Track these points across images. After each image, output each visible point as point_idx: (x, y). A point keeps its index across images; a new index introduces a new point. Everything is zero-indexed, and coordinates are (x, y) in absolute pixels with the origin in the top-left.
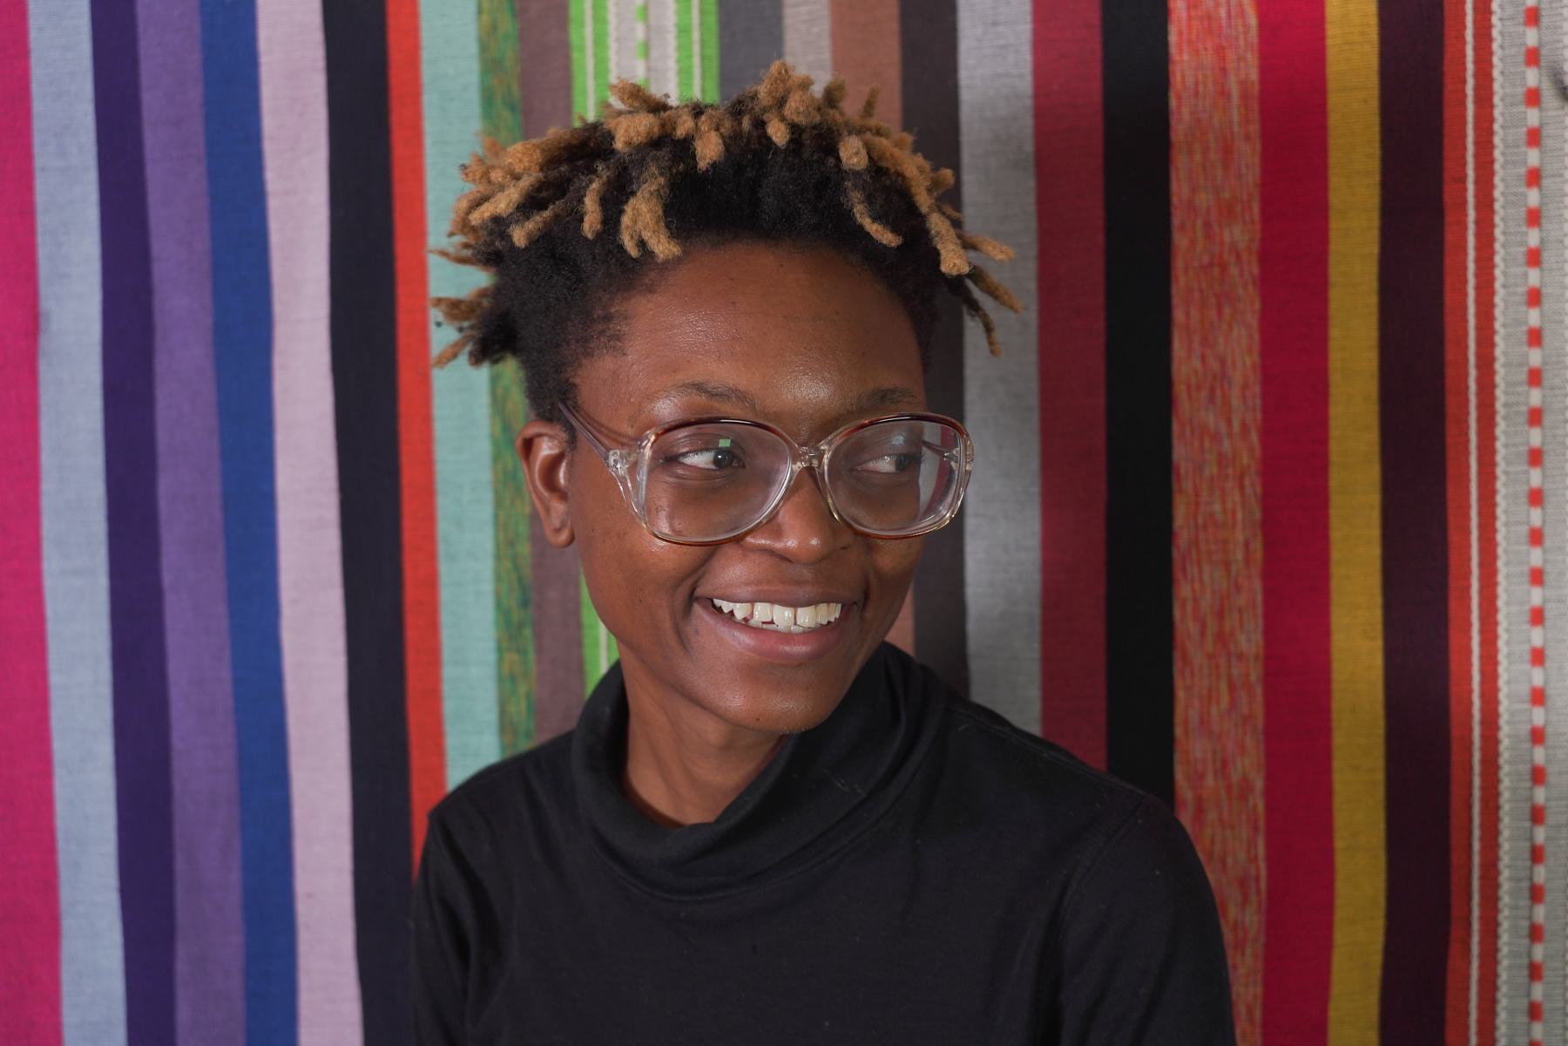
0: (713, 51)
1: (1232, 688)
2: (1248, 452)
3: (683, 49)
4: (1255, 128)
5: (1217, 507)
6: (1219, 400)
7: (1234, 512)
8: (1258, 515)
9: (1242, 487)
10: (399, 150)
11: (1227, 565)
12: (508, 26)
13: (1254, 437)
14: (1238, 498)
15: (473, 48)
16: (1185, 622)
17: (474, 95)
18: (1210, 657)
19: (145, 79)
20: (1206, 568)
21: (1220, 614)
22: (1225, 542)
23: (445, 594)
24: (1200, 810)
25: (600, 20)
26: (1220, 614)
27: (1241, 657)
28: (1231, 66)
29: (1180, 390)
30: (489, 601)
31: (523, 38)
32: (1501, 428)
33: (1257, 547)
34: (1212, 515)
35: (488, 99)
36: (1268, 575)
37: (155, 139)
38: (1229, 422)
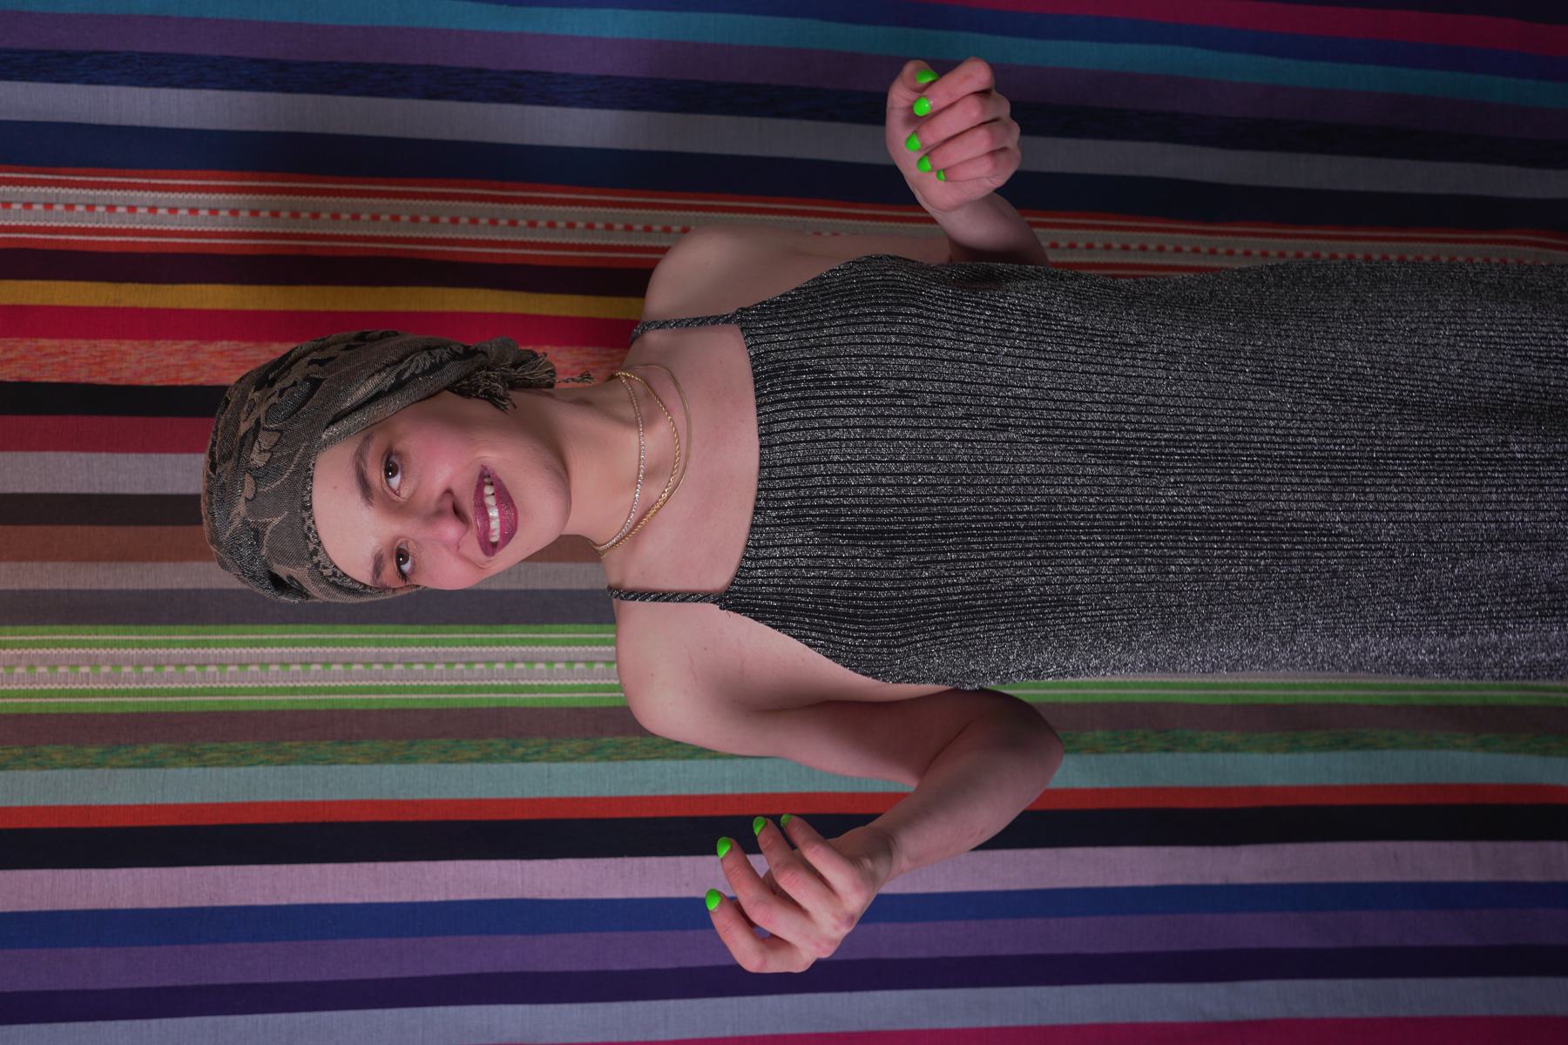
0: (392, 627)
10: (428, 816)
12: (366, 745)
13: (614, 351)
15: (376, 767)
17: (402, 768)
23: (684, 791)
25: (369, 690)
30: (689, 763)
32: (613, 242)
37: (409, 970)
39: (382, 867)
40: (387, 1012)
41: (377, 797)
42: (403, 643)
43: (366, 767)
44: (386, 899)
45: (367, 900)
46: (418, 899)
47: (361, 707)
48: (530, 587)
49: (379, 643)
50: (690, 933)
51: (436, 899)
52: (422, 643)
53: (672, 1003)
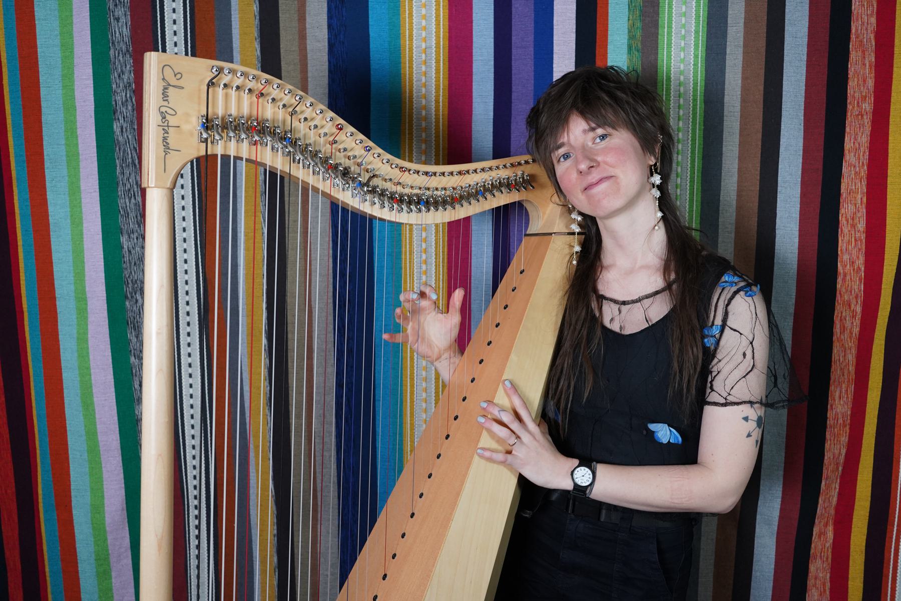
0: (705, 39)
1: (856, 240)
2: (864, 172)
3: (697, 38)
4: (873, 75)
11: (855, 205)
12: (639, 24)
15: (626, 31)
16: (842, 220)
17: (625, 47)
19: (513, 33)
21: (853, 219)
24: (845, 275)
26: (853, 219)
28: (867, 56)
29: (846, 152)
31: (643, 29)
33: (865, 200)
35: (630, 48)
36: (867, 208)
39: (574, 36)
40: (492, 40)
41: (609, 33)
42: (696, 46)
43: (626, 26)
44: (555, 38)
45: (555, 27)
46: (555, 56)
47: (660, 23)
48: (725, 118)
49: (697, 32)
51: (554, 66)
52: (696, 56)
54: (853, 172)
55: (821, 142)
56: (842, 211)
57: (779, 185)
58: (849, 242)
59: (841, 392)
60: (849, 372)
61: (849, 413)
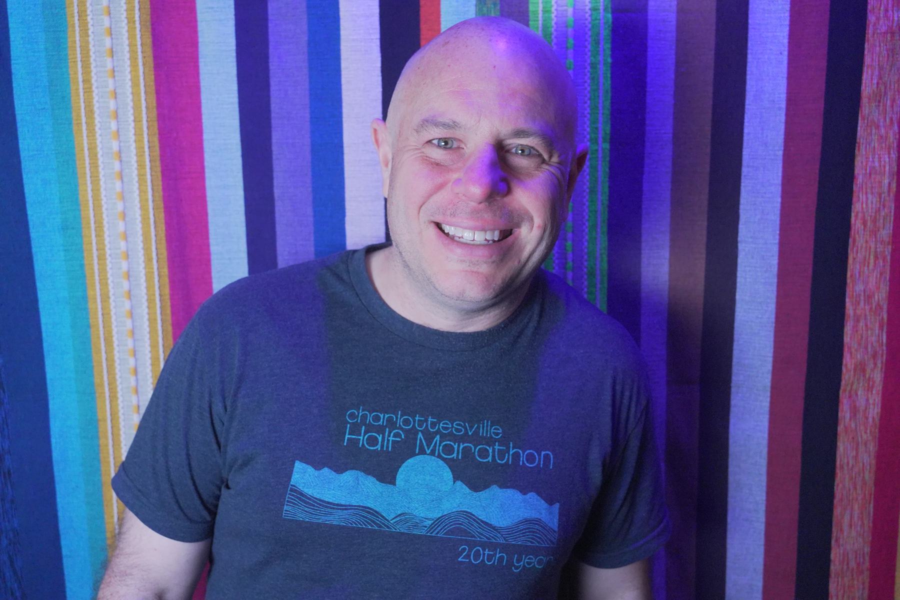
5: (877, 164)
6: (881, 108)
7: (885, 167)
8: (895, 169)
9: (889, 154)
11: (880, 195)
13: (896, 128)
14: (887, 160)
16: (856, 223)
18: (867, 242)
20: (870, 196)
22: (880, 182)
26: (875, 221)
27: (882, 242)
33: (894, 185)
34: (873, 168)
38: (885, 120)
50: (310, 211)
53: (241, 193)
54: (875, 137)
55: (820, 84)
56: (857, 207)
57: (744, 163)
58: (865, 262)
59: (852, 517)
60: (864, 483)
61: (867, 549)
